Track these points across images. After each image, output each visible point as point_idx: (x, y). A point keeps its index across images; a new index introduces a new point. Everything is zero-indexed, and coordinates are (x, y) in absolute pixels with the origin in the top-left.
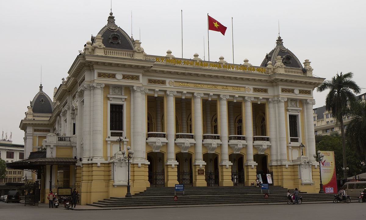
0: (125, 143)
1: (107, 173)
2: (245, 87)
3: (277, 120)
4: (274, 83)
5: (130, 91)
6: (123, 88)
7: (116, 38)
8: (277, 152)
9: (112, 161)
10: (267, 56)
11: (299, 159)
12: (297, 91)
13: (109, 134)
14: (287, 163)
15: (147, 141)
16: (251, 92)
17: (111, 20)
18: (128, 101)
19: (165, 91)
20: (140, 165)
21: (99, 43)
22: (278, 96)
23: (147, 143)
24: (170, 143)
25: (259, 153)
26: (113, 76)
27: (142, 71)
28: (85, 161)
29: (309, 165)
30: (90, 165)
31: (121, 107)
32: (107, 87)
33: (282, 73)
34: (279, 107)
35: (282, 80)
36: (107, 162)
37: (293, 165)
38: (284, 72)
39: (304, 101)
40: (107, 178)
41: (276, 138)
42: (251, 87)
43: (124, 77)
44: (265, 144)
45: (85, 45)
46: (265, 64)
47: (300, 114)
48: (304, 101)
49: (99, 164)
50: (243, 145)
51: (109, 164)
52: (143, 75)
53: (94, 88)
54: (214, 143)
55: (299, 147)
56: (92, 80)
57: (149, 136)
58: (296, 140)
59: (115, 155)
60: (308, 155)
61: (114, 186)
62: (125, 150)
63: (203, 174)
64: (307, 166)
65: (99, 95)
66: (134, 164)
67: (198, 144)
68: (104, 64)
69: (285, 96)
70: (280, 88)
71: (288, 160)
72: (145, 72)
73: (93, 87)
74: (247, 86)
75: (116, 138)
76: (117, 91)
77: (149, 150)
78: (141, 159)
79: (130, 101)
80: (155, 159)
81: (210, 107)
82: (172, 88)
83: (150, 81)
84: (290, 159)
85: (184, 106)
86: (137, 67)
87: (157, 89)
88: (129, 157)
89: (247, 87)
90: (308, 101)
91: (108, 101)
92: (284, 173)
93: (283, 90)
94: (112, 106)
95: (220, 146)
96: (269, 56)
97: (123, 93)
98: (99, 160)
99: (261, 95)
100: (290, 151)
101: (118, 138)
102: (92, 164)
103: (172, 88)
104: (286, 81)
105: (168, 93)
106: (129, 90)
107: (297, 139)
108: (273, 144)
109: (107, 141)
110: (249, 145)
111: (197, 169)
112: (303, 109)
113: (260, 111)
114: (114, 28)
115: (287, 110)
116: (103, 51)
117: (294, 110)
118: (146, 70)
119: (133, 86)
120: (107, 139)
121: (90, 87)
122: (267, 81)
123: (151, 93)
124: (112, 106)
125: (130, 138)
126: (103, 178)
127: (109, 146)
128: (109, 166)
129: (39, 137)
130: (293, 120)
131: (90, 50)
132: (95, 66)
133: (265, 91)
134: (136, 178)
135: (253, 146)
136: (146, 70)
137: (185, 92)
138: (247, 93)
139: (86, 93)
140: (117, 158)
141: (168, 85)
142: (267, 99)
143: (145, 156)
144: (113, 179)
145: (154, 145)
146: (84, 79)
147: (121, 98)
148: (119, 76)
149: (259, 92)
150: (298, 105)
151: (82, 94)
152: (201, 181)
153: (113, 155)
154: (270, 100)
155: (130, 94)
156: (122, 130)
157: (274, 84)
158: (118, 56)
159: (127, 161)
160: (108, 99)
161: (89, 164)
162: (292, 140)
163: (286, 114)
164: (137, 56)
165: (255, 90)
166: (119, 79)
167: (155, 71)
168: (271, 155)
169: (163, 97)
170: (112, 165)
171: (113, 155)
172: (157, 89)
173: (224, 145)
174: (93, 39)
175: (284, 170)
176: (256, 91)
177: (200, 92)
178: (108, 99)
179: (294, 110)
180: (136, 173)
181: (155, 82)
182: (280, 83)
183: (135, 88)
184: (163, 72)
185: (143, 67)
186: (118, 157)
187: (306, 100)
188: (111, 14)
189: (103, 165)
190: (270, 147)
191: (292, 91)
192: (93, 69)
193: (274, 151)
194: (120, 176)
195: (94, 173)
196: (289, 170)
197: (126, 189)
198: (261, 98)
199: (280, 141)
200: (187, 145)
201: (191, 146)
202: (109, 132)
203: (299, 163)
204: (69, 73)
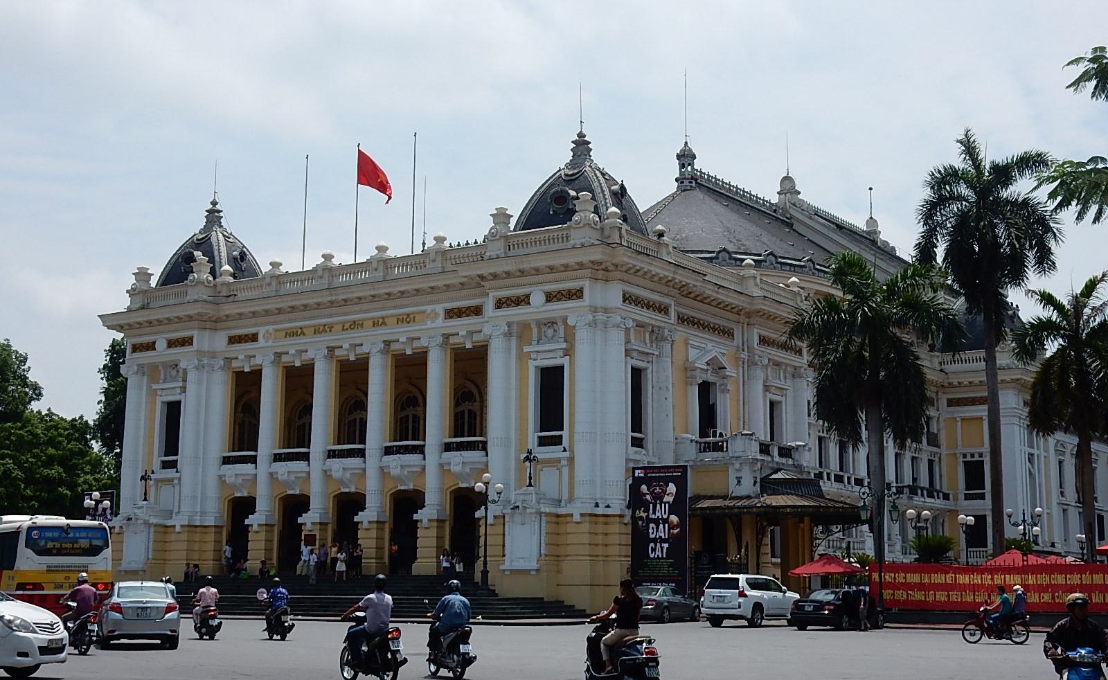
16: (440, 321)
35: (482, 277)
42: (440, 309)
50: (402, 466)
57: (227, 461)
58: (557, 441)
74: (429, 308)
89: (429, 311)
93: (500, 304)
99: (461, 326)
113: (470, 369)
115: (523, 358)
148: (161, 345)
149: (459, 317)
165: (451, 314)
176: (451, 317)
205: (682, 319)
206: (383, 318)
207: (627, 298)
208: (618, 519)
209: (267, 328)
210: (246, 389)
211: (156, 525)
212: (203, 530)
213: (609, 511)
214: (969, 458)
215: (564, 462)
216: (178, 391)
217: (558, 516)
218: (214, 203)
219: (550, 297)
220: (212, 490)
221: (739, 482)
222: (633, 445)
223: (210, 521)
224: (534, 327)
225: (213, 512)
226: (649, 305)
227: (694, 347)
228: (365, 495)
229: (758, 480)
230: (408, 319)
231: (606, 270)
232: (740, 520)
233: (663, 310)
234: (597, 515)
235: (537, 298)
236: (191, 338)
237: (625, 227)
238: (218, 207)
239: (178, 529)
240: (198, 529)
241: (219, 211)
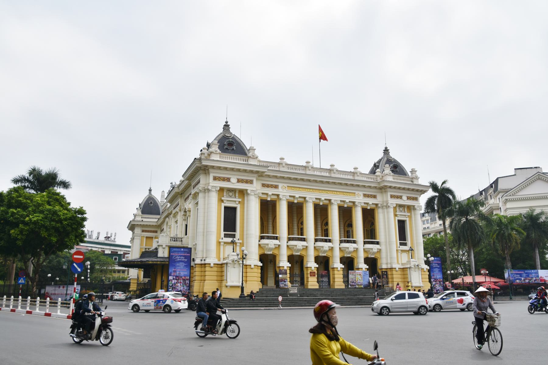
0: (238, 244)
1: (219, 274)
3: (387, 226)
4: (383, 189)
5: (244, 195)
6: (237, 192)
7: (231, 144)
8: (387, 256)
9: (225, 262)
10: (375, 164)
11: (409, 262)
12: (405, 198)
13: (222, 236)
15: (260, 243)
17: (227, 128)
18: (242, 203)
19: (278, 195)
20: (252, 266)
21: (215, 148)
22: (387, 202)
23: (259, 245)
24: (283, 246)
25: (369, 256)
26: (228, 180)
27: (256, 175)
28: (198, 261)
29: (419, 268)
30: (203, 266)
31: (235, 209)
32: (222, 190)
33: (390, 180)
34: (388, 212)
35: (390, 187)
36: (220, 263)
37: (403, 269)
38: (392, 180)
39: (412, 207)
40: (219, 278)
41: (386, 242)
42: (361, 193)
43: (239, 181)
44: (375, 247)
45: (201, 151)
46: (373, 172)
47: (407, 219)
48: (412, 207)
49: (212, 265)
51: (222, 264)
52: (257, 180)
53: (209, 190)
54: (326, 246)
55: (408, 251)
56: (207, 182)
57: (262, 238)
58: (405, 244)
59: (228, 255)
60: (416, 258)
61: (227, 286)
62: (238, 251)
63: (315, 276)
64: (417, 270)
65: (214, 197)
66: (246, 265)
67: (310, 247)
68: (219, 168)
69: (394, 202)
70: (389, 194)
71: (398, 263)
72: (259, 176)
73: (208, 189)
74: (357, 192)
75: (229, 240)
76: (231, 194)
77: (262, 252)
78: (254, 260)
79: (244, 204)
80: (268, 261)
81: (321, 212)
82: (284, 193)
83: (264, 185)
84: (400, 262)
85: (296, 210)
86: (252, 172)
87: (270, 193)
88: (244, 258)
90: (416, 207)
91: (222, 204)
92: (394, 276)
94: (226, 208)
95: (332, 249)
96: (377, 164)
97: (237, 195)
98: (212, 260)
99: (371, 201)
100: (399, 254)
101: (232, 239)
102: (205, 264)
103: (284, 193)
104: (395, 188)
105: (281, 196)
106: (243, 193)
107: (406, 243)
108: (382, 247)
109: (220, 242)
110: (359, 248)
111: (309, 271)
112: (411, 214)
113: (369, 215)
114: (229, 135)
115: (396, 215)
116: (218, 156)
117: (403, 215)
118: (260, 175)
119: (247, 190)
120: (221, 240)
121: (205, 190)
122: (376, 187)
123: (264, 197)
124: (226, 208)
125: (243, 241)
126: (215, 278)
127: (222, 247)
128: (221, 267)
129: (147, 237)
130: (402, 225)
131: (206, 155)
132: (211, 170)
133: (375, 197)
134: (248, 279)
135: (364, 249)
136: (260, 175)
137: (297, 196)
139: (201, 195)
140: (230, 259)
141: (280, 189)
142: (377, 205)
143: (257, 257)
144: (226, 280)
145: (267, 247)
146: (199, 182)
147: (235, 201)
148: (234, 180)
150: (406, 210)
151: (196, 195)
152: (312, 283)
153: (226, 256)
154: (379, 205)
155: (244, 197)
156: (235, 232)
157: (383, 190)
158: (232, 160)
159: (241, 262)
160: (222, 201)
161: (202, 264)
162: (401, 244)
163: (395, 219)
164: (251, 162)
165: (365, 195)
166: (234, 184)
167: (269, 176)
168: (381, 258)
169: (276, 201)
170: (225, 265)
171: (226, 256)
172: (270, 193)
173: (335, 248)
174: (208, 145)
175: (394, 272)
177: (312, 197)
178: (222, 201)
179: (403, 215)
180: (248, 274)
181: (268, 186)
182: (389, 190)
183: (249, 192)
184: (276, 177)
185: (257, 172)
186: (231, 258)
187: (414, 206)
188: (227, 122)
189: (216, 266)
190: (379, 251)
191: (401, 197)
192: (209, 173)
193: (384, 254)
194: (234, 277)
195: (207, 273)
196: (399, 272)
197: (240, 290)
198: (371, 203)
199: (390, 244)
200: (299, 248)
201: (303, 249)
202: (223, 233)
203: (409, 266)
204: (183, 176)
209: (283, 184)
210: (268, 209)
216: (237, 203)
219: (408, 198)
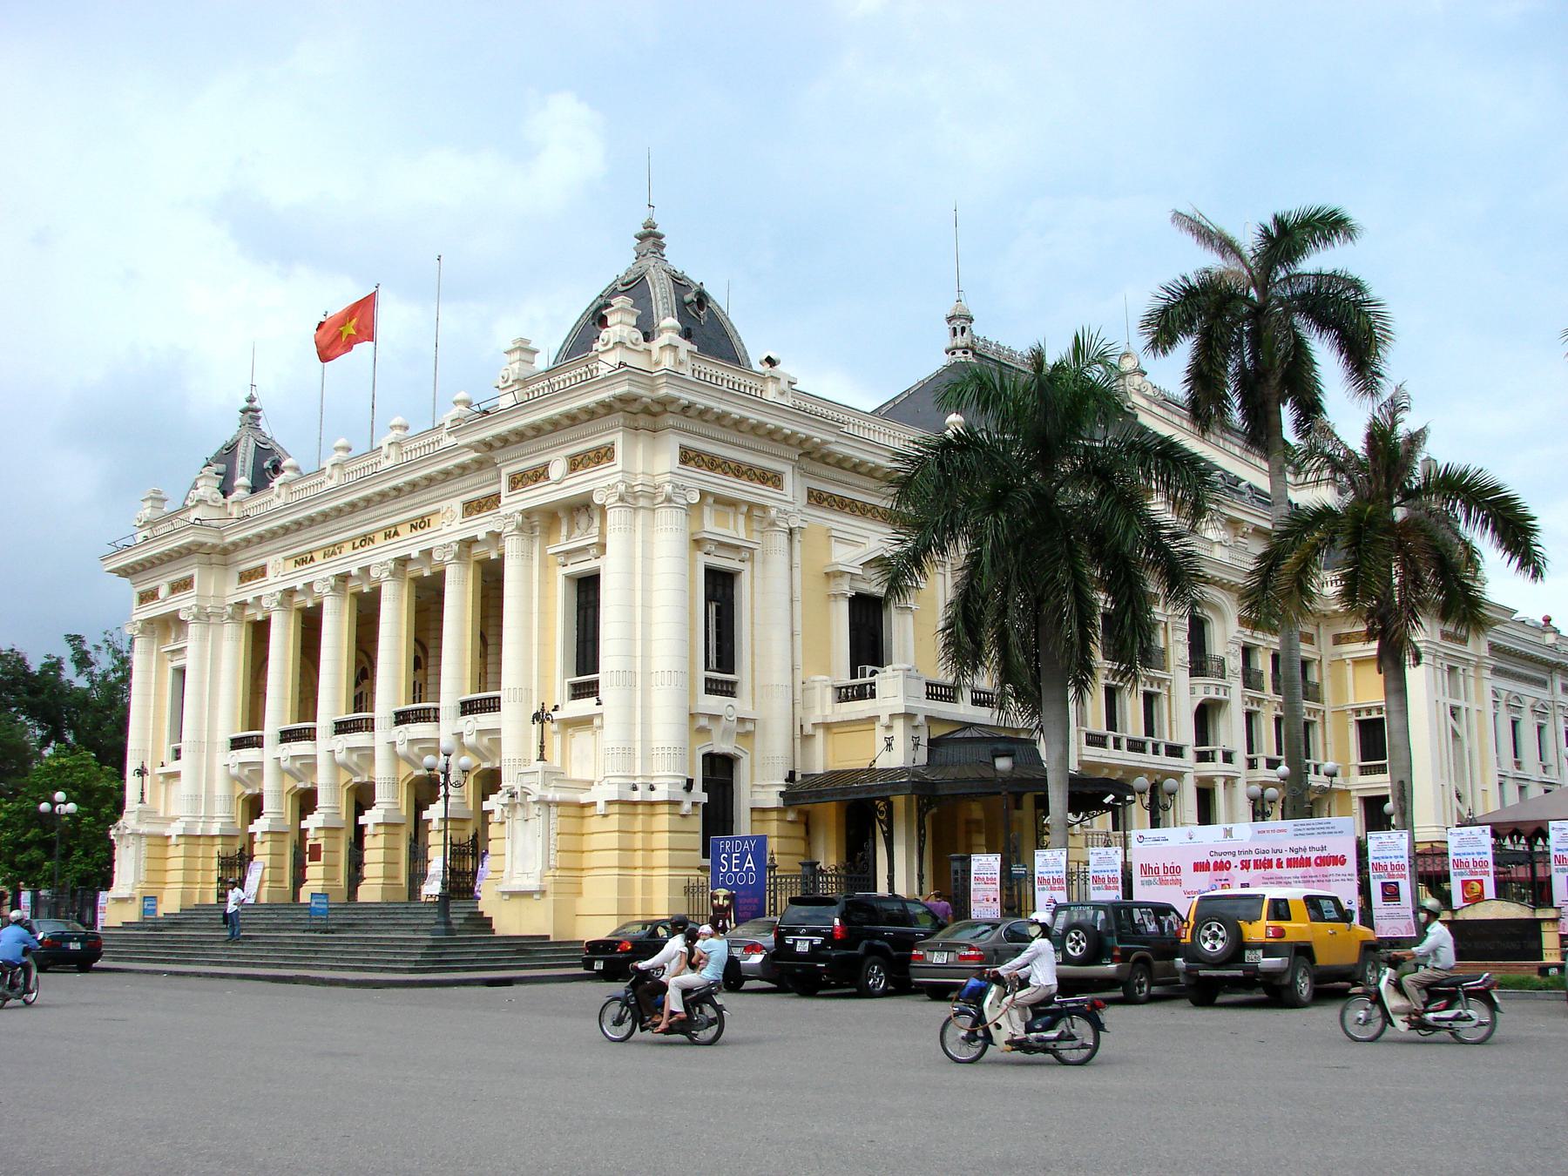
2: (437, 512)
14: (601, 794)
35: (488, 445)
42: (456, 505)
57: (237, 744)
74: (444, 505)
93: (516, 482)
99: (480, 526)
138: (446, 530)
165: (472, 508)
182: (498, 456)
205: (817, 498)
206: (395, 526)
207: (687, 456)
208: (666, 808)
211: (148, 836)
212: (208, 841)
213: (655, 796)
214: (1364, 716)
215: (597, 722)
217: (583, 806)
218: (251, 400)
220: (220, 788)
221: (889, 745)
222: (708, 691)
223: (215, 830)
224: (561, 514)
225: (220, 817)
226: (739, 471)
227: (839, 540)
228: (373, 785)
229: (924, 741)
230: (420, 523)
231: (647, 411)
232: (890, 805)
233: (774, 480)
234: (635, 803)
235: (558, 469)
236: (191, 577)
237: (685, 345)
238: (256, 404)
239: (173, 840)
240: (201, 841)
241: (257, 411)
